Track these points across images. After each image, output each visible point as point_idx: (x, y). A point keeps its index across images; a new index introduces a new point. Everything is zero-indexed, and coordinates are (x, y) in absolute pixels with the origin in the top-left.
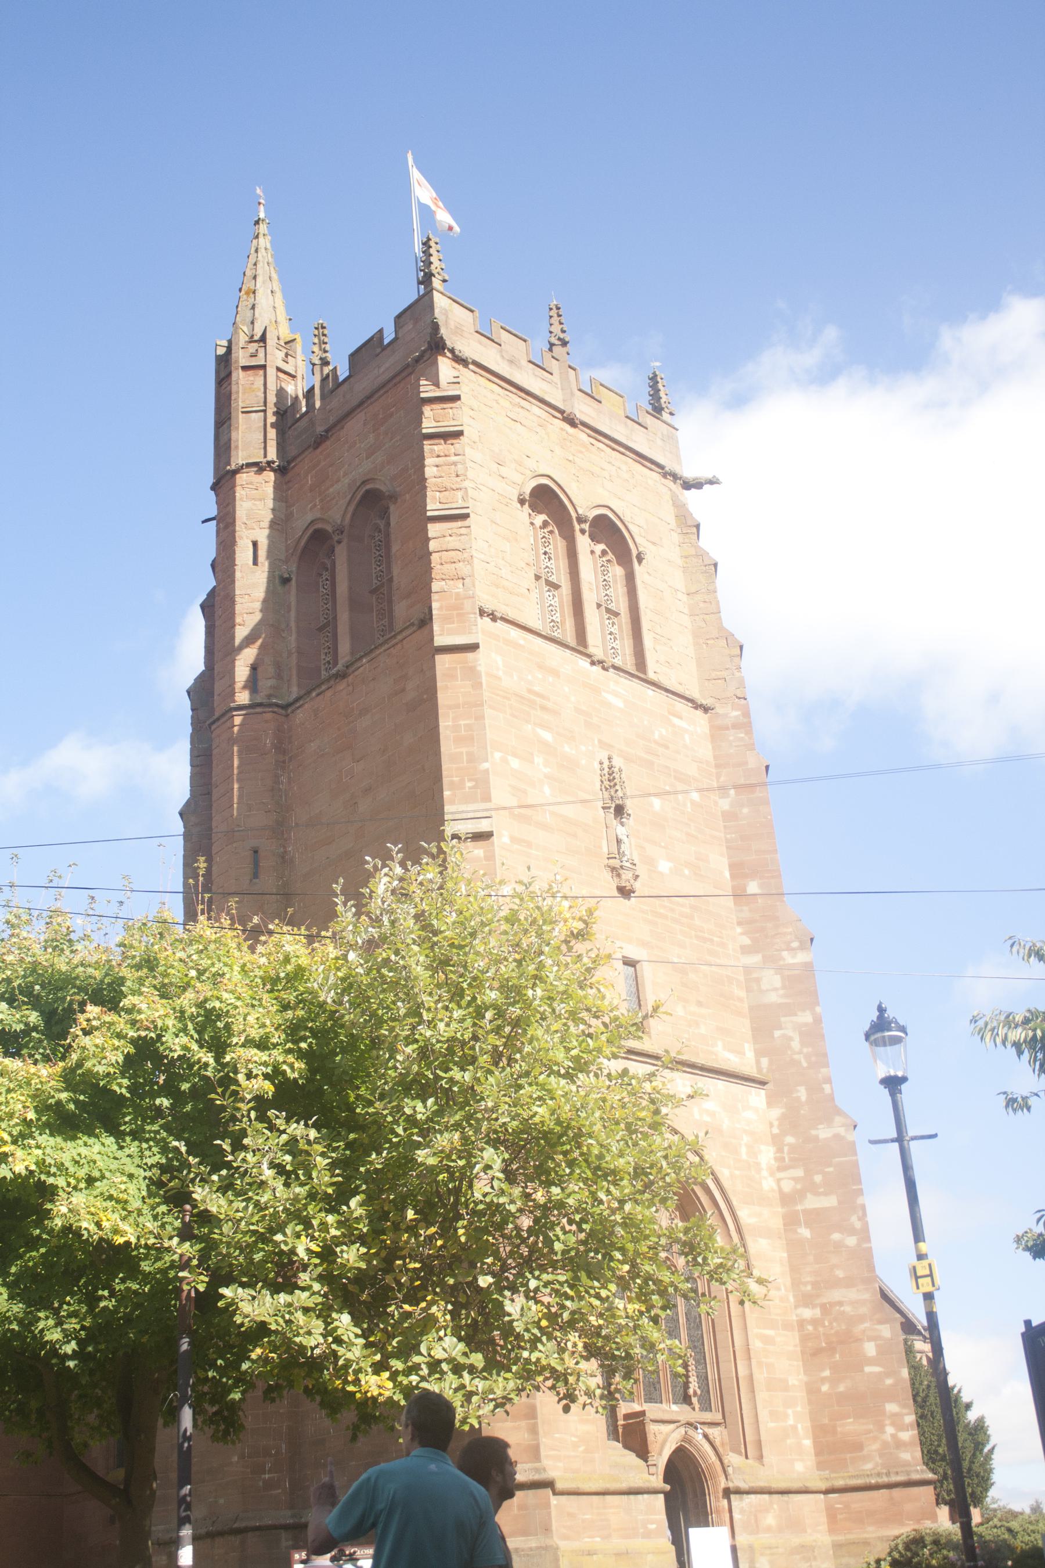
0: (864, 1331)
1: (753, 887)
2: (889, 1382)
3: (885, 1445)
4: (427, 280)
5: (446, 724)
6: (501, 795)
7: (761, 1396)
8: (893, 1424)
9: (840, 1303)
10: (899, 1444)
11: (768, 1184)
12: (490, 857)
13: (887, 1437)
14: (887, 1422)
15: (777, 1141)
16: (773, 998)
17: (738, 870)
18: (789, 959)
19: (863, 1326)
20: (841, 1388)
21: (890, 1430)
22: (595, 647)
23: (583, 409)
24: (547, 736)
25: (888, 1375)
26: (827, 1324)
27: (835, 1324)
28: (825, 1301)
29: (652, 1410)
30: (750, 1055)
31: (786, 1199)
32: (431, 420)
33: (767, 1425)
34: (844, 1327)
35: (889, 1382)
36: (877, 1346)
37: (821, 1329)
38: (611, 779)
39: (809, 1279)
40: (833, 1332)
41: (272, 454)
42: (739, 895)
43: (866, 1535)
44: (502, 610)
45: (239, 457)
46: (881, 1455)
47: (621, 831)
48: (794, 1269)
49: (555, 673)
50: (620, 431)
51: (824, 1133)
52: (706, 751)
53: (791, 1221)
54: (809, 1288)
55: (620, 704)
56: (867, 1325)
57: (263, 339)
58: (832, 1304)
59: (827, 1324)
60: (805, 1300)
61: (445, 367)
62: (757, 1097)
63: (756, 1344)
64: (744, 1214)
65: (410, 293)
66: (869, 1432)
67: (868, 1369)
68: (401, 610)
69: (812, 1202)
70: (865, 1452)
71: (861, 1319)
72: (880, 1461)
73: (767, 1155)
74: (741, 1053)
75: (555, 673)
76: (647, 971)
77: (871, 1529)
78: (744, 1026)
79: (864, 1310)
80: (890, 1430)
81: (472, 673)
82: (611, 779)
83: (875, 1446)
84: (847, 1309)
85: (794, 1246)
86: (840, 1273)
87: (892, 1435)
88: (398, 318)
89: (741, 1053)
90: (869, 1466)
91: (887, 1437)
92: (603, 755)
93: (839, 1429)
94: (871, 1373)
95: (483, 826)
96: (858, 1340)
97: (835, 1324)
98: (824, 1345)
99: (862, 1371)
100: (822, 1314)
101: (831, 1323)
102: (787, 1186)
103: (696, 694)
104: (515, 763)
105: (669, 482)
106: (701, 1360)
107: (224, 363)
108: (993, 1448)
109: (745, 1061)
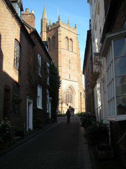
1: (79, 68)
4: (59, 19)
5: (59, 58)
6: (62, 63)
7: (75, 103)
10: (84, 106)
11: (77, 89)
12: (61, 68)
15: (78, 86)
16: (79, 76)
17: (78, 67)
18: (81, 73)
22: (69, 50)
23: (70, 29)
24: (65, 57)
29: (69, 103)
30: (77, 80)
31: (78, 90)
32: (59, 33)
33: (76, 105)
38: (69, 60)
41: (46, 31)
42: (78, 68)
44: (63, 48)
45: (43, 31)
47: (70, 64)
48: (78, 95)
49: (66, 52)
50: (72, 31)
51: (81, 86)
52: (76, 57)
53: (79, 92)
55: (70, 54)
57: (45, 19)
60: (79, 97)
61: (60, 27)
62: (77, 83)
63: (75, 100)
64: (75, 91)
65: (58, 20)
68: (56, 47)
69: (80, 90)
73: (77, 87)
74: (76, 80)
75: (66, 52)
76: (71, 75)
78: (77, 78)
81: (61, 54)
82: (69, 60)
85: (79, 93)
88: (57, 22)
89: (76, 80)
92: (69, 58)
95: (61, 66)
102: (79, 89)
103: (76, 53)
104: (63, 60)
105: (76, 35)
106: (72, 101)
107: (42, 20)
109: (77, 80)
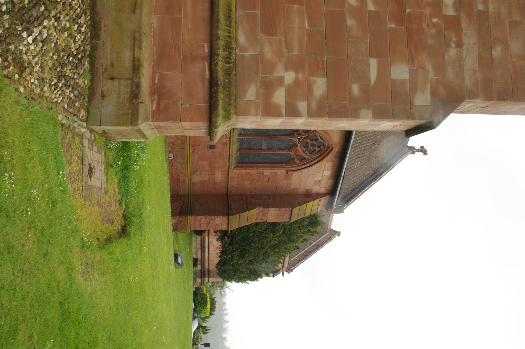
0: (424, 68)
2: (356, 89)
3: (270, 67)
8: (297, 83)
9: (459, 44)
13: (279, 72)
14: (300, 76)
19: (429, 67)
20: (350, 22)
21: (289, 77)
25: (366, 90)
26: (435, 20)
27: (433, 31)
28: (464, 22)
34: (429, 42)
35: (356, 89)
36: (404, 81)
37: (427, 11)
39: (491, 9)
40: (424, 26)
43: (145, 11)
46: (255, 57)
54: (480, 7)
56: (431, 75)
58: (459, 31)
59: (435, 20)
66: (289, 49)
67: (374, 63)
70: (261, 36)
71: (440, 69)
72: (247, 54)
77: (155, 21)
79: (451, 74)
80: (289, 77)
83: (268, 53)
84: (452, 52)
86: (497, 52)
87: (281, 80)
90: (242, 39)
91: (279, 72)
93: (295, 7)
94: (369, 66)
96: (412, 60)
97: (433, 31)
98: (408, 11)
99: (372, 56)
100: (447, 17)
101: (435, 25)
108: (248, 283)
